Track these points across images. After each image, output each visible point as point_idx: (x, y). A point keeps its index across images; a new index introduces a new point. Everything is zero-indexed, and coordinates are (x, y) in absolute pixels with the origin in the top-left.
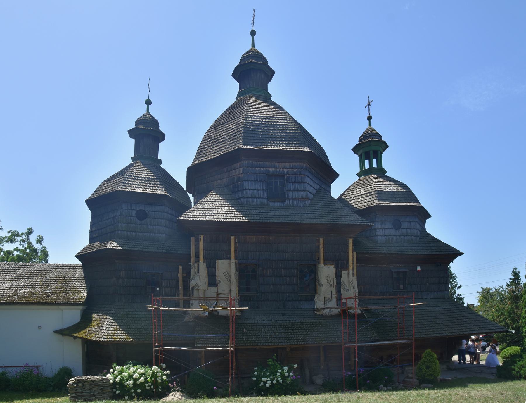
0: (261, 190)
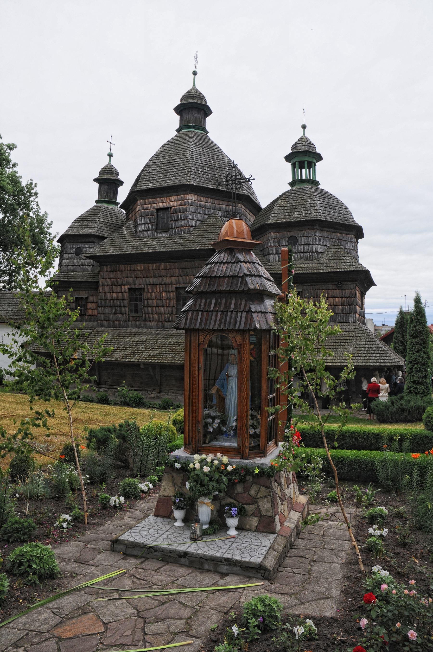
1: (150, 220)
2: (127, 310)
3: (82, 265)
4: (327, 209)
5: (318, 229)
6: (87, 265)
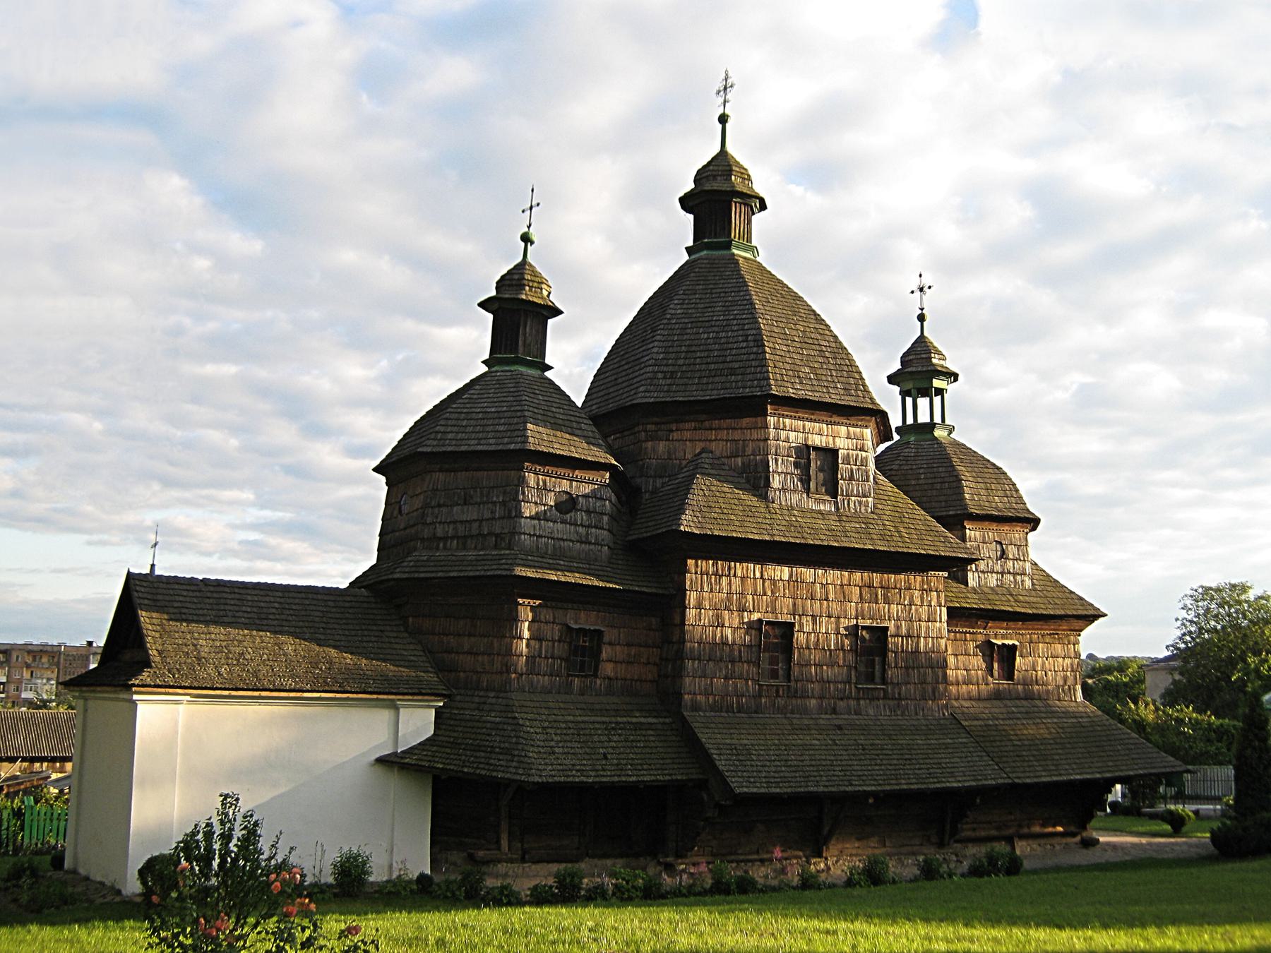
3: (582, 542)
6: (594, 544)
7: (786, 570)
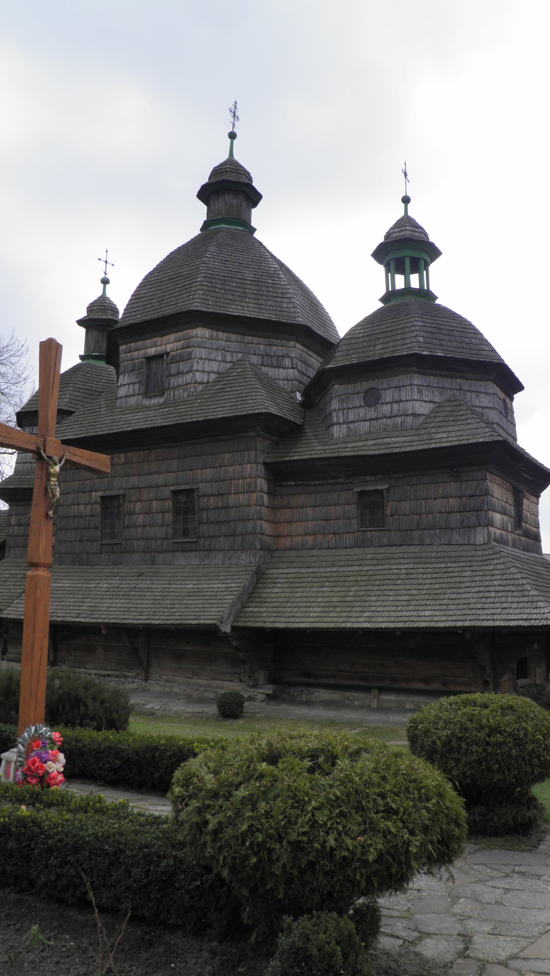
0: (137, 383)
1: (137, 378)
2: (98, 533)
4: (435, 336)
5: (416, 373)
7: (122, 456)
